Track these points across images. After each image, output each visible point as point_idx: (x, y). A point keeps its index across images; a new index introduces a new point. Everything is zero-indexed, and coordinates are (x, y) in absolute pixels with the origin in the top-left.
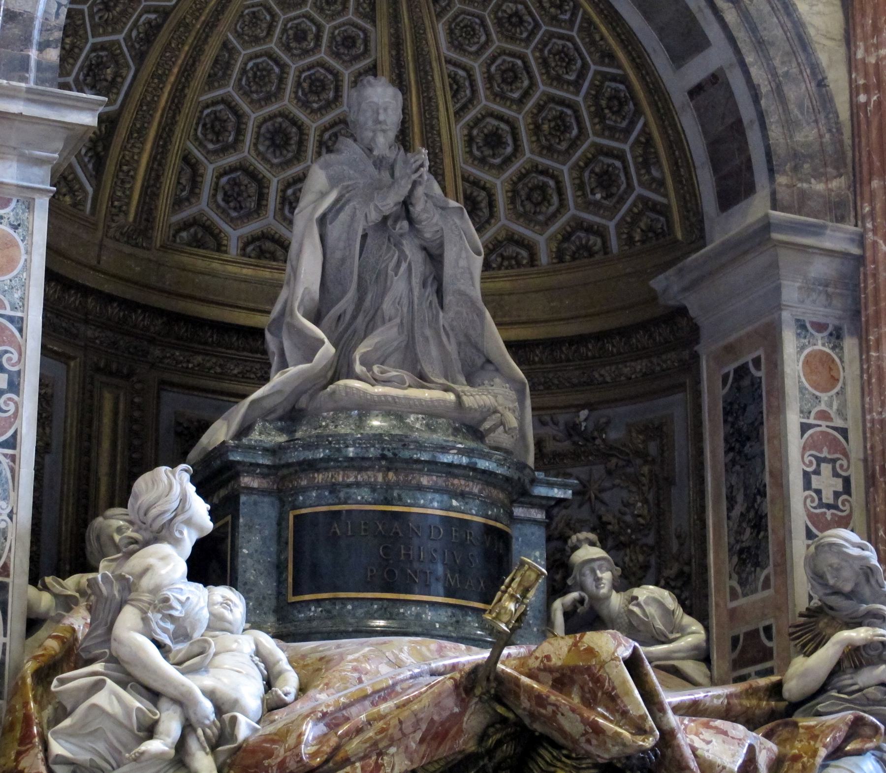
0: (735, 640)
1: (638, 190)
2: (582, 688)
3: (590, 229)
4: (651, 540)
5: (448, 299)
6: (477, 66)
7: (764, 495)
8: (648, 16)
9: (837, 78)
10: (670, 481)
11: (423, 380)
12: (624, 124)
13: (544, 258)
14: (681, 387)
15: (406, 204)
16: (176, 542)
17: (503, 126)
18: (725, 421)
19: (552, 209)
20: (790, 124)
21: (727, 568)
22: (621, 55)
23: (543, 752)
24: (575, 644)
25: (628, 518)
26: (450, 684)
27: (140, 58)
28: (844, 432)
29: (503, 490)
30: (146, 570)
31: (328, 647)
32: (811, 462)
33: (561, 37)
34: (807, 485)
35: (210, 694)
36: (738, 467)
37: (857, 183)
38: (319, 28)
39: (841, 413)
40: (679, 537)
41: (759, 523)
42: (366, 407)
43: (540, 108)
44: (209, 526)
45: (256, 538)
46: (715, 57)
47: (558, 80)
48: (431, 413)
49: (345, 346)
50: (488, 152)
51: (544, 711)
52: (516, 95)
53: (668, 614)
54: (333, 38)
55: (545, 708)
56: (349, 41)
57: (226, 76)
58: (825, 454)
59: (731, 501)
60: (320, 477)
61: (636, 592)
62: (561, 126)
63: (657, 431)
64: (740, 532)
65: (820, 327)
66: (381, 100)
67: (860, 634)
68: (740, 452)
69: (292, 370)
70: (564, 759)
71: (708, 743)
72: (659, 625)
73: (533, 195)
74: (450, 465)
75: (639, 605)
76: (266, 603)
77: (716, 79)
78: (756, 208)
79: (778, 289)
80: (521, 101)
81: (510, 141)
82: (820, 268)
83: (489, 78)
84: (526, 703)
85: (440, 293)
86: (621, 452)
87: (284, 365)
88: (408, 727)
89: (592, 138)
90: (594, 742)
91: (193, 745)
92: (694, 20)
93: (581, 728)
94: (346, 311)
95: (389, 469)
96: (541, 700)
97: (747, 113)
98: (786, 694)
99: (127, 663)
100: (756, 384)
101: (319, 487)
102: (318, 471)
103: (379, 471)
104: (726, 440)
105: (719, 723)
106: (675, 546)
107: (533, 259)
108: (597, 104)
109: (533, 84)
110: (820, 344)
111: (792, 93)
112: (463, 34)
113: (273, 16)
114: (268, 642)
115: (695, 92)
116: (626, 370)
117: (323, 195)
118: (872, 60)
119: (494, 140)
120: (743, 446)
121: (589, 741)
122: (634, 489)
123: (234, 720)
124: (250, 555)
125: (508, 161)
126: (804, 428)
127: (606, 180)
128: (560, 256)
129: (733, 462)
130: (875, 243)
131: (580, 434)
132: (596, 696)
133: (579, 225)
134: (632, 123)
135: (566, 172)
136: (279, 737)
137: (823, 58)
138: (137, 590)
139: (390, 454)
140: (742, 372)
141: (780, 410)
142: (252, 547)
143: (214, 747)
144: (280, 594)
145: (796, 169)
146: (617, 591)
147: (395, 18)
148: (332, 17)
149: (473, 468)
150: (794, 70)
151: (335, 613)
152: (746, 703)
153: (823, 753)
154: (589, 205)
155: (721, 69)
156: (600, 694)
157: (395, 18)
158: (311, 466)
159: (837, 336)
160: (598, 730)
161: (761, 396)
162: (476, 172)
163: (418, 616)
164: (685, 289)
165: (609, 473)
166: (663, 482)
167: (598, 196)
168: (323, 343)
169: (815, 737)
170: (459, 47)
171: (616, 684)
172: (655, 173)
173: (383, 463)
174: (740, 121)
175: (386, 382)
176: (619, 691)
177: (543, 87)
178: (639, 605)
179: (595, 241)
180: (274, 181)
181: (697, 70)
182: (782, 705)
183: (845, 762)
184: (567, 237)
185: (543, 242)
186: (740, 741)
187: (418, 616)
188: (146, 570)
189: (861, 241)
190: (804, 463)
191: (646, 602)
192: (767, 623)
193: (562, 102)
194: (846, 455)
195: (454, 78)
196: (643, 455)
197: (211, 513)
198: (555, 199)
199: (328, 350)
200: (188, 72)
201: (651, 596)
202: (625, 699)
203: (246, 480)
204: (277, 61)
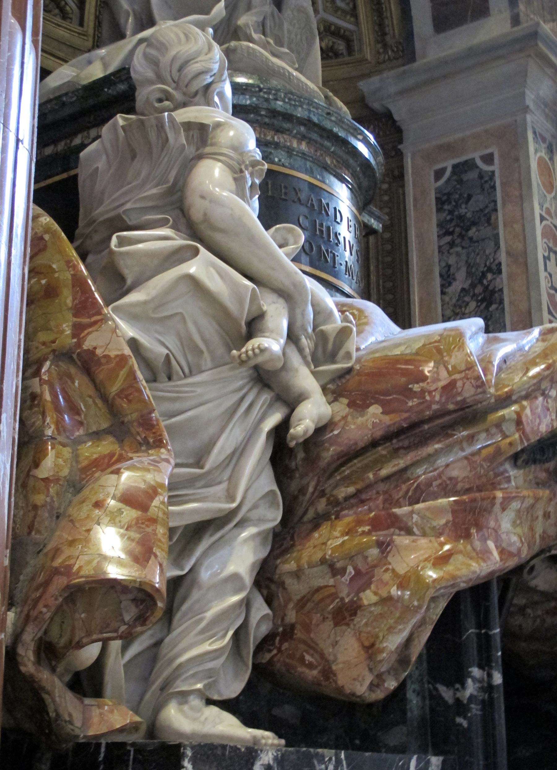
7: (500, 272)
18: (439, 210)
36: (459, 249)
59: (447, 278)
68: (462, 236)
99: (223, 231)
104: (440, 225)
120: (467, 230)
126: (542, 219)
129: (452, 244)
138: (212, 145)
139: (315, 119)
161: (494, 187)
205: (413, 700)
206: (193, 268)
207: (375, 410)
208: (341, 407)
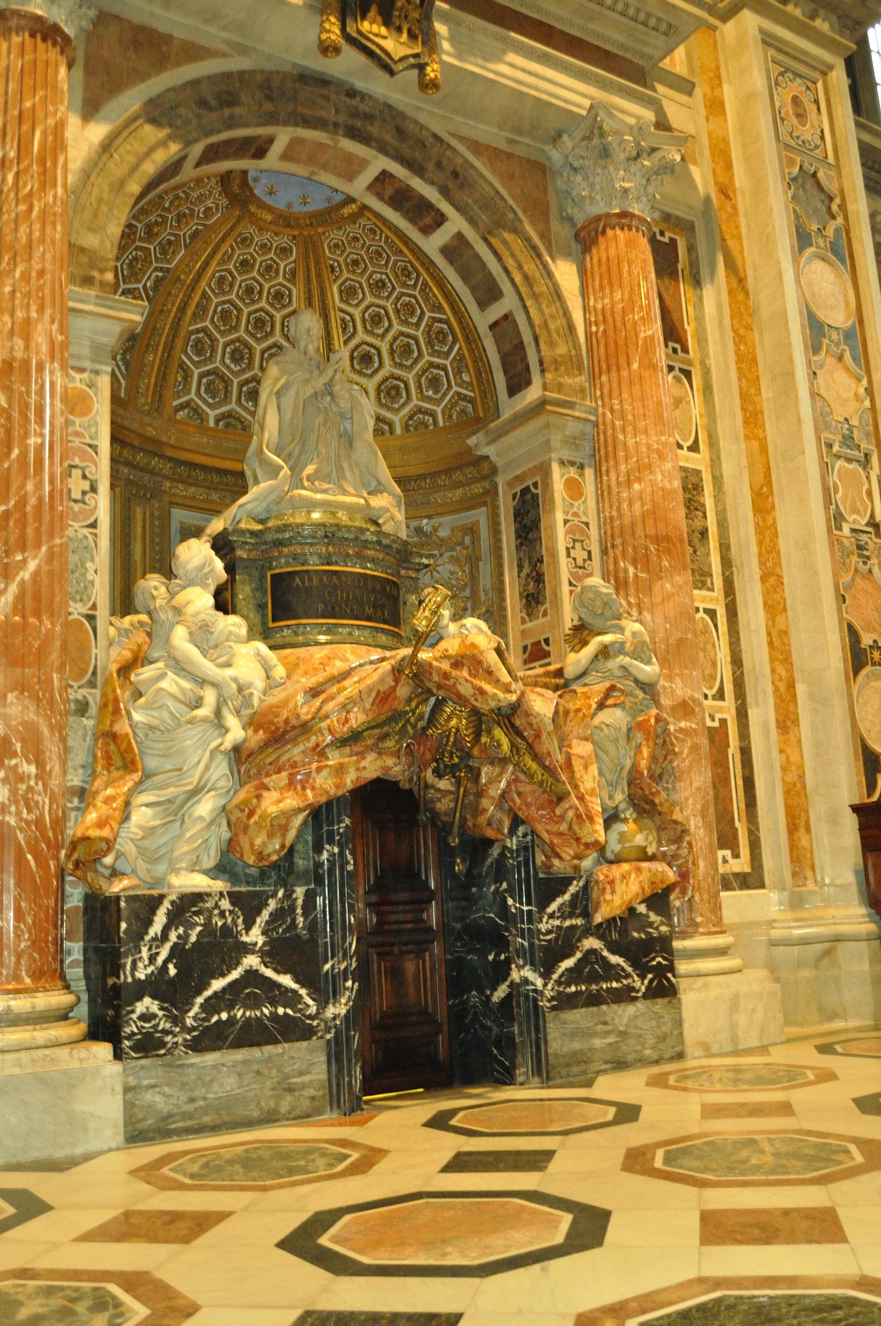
0: (525, 648)
1: (455, 388)
3: (426, 412)
4: (467, 593)
6: (357, 313)
8: (465, 278)
10: (479, 559)
11: (344, 492)
12: (446, 349)
13: (398, 430)
14: (485, 504)
15: (330, 384)
16: (205, 586)
17: (373, 351)
19: (402, 401)
21: (518, 606)
22: (445, 305)
26: (389, 667)
28: (587, 524)
30: (189, 603)
31: (302, 652)
33: (409, 295)
34: (569, 555)
35: (235, 680)
37: (592, 377)
38: (261, 285)
41: (539, 579)
42: (313, 505)
43: (395, 339)
44: (224, 576)
45: (248, 589)
46: (508, 303)
47: (406, 323)
48: (351, 509)
49: (296, 469)
52: (380, 331)
54: (269, 293)
56: (279, 296)
57: (205, 315)
58: (577, 537)
59: (520, 567)
60: (285, 550)
61: (464, 621)
62: (406, 350)
63: (472, 530)
64: (527, 585)
65: (572, 464)
66: (309, 323)
67: (608, 638)
69: (263, 485)
73: (389, 393)
74: (366, 541)
77: (507, 317)
78: (533, 393)
79: (548, 440)
80: (383, 336)
81: (376, 358)
82: (572, 428)
83: (364, 320)
84: (436, 678)
87: (257, 482)
88: (364, 696)
91: (225, 712)
92: (494, 280)
93: (472, 691)
94: (295, 450)
96: (446, 676)
97: (527, 337)
98: (566, 675)
100: (535, 497)
101: (286, 556)
105: (538, 690)
106: (482, 594)
107: (392, 431)
108: (429, 336)
109: (390, 325)
110: (573, 472)
111: (552, 326)
112: (348, 293)
113: (233, 277)
114: (262, 647)
115: (493, 327)
117: (277, 380)
118: (599, 306)
119: (366, 359)
123: (251, 694)
125: (375, 372)
126: (566, 522)
127: (434, 383)
128: (406, 427)
129: (521, 544)
130: (604, 414)
131: (425, 534)
133: (420, 410)
134: (451, 348)
135: (410, 377)
136: (285, 703)
140: (525, 491)
141: (552, 510)
142: (244, 592)
143: (238, 713)
144: (264, 623)
145: (556, 370)
147: (308, 281)
148: (269, 280)
149: (379, 542)
150: (554, 311)
152: (545, 680)
153: (594, 706)
154: (424, 398)
155: (511, 312)
157: (308, 281)
158: (279, 543)
159: (582, 467)
160: (482, 692)
163: (350, 634)
164: (489, 443)
166: (473, 560)
169: (589, 698)
170: (347, 302)
172: (466, 377)
174: (522, 343)
175: (324, 491)
177: (397, 327)
180: (236, 381)
181: (495, 312)
182: (562, 681)
183: (606, 711)
184: (411, 418)
186: (552, 700)
187: (350, 634)
188: (189, 603)
193: (409, 336)
195: (343, 320)
196: (461, 544)
197: (226, 568)
198: (404, 394)
199: (286, 471)
200: (183, 309)
204: (235, 306)
205: (300, 863)
206: (164, 684)
207: (261, 732)
208: (250, 732)
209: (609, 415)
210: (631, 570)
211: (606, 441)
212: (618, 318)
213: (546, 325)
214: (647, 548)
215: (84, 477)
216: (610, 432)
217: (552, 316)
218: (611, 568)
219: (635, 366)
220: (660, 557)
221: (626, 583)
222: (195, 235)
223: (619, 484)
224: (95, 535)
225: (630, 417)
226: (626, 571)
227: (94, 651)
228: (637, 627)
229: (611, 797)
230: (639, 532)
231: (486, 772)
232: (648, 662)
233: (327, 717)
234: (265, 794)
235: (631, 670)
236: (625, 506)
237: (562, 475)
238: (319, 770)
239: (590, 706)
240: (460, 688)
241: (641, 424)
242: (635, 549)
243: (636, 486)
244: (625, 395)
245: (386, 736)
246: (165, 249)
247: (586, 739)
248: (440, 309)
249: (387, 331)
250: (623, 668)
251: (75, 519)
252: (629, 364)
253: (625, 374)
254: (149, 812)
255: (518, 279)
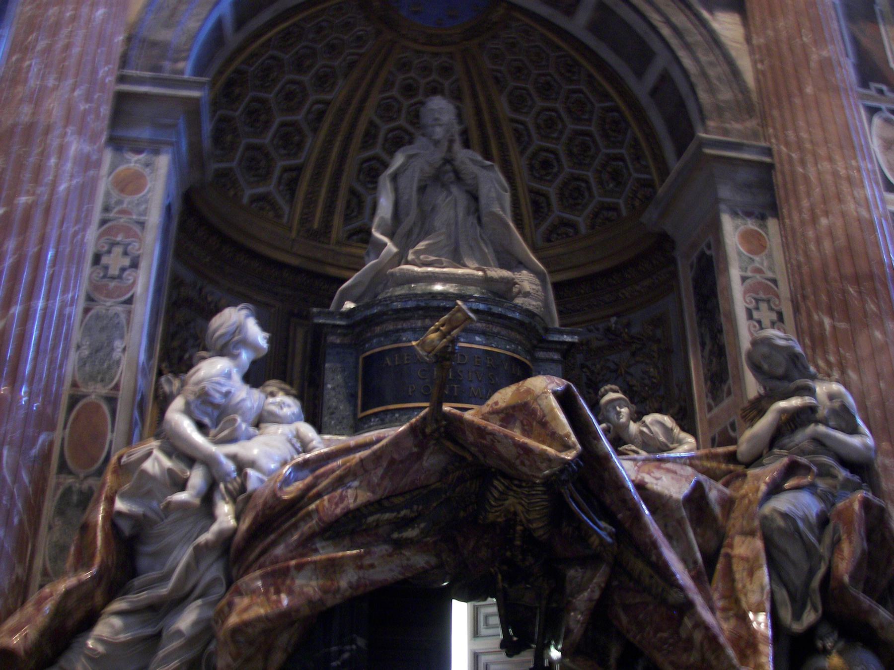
2: (522, 422)
5: (484, 219)
6: (529, 120)
9: (745, 64)
13: (583, 229)
15: (448, 161)
20: (712, 90)
21: (704, 390)
23: (496, 483)
24: (518, 389)
25: (647, 381)
27: (315, 130)
28: (774, 281)
29: (520, 333)
32: (751, 302)
34: (750, 317)
35: (234, 458)
39: (770, 269)
40: (677, 385)
43: (570, 140)
45: (339, 377)
50: (543, 172)
51: (484, 442)
53: (668, 431)
55: (485, 438)
58: (762, 295)
59: (703, 345)
60: (378, 329)
64: (711, 361)
66: (441, 110)
70: (515, 488)
71: (657, 479)
72: (662, 438)
75: (646, 426)
76: (345, 421)
81: (555, 163)
82: (744, 175)
83: (538, 127)
85: (479, 219)
86: (638, 339)
89: (604, 151)
90: (527, 463)
95: (425, 317)
97: (684, 89)
98: (739, 457)
102: (377, 324)
103: (418, 319)
110: (751, 225)
111: (711, 72)
112: (518, 102)
116: (638, 288)
119: (546, 165)
121: (522, 463)
122: (648, 361)
124: (333, 389)
125: (556, 175)
126: (744, 279)
127: (616, 176)
128: (593, 227)
132: (532, 426)
133: (604, 207)
135: (590, 175)
137: (733, 53)
141: (726, 270)
143: (233, 497)
146: (635, 422)
147: (475, 96)
151: (387, 420)
153: (763, 488)
156: (534, 424)
162: (536, 185)
165: (633, 354)
167: (611, 185)
168: (386, 245)
170: (516, 110)
171: (546, 411)
172: (643, 163)
173: (420, 312)
176: (548, 418)
178: (646, 426)
179: (612, 215)
181: (651, 77)
184: (596, 215)
185: (581, 220)
189: (769, 152)
190: (746, 302)
191: (651, 424)
192: (731, 420)
194: (778, 296)
195: (516, 130)
201: (657, 422)
202: (553, 424)
203: (332, 339)
209: (783, 149)
210: (827, 321)
211: (784, 180)
212: (785, 48)
213: (704, 74)
214: (844, 291)
215: (125, 253)
216: (787, 167)
217: (711, 64)
218: (805, 323)
219: (809, 90)
220: (863, 301)
221: (823, 339)
222: (352, 65)
223: (803, 223)
224: (129, 313)
225: (808, 146)
226: (821, 324)
227: (109, 437)
228: (836, 387)
229: (797, 616)
230: (833, 274)
231: (574, 573)
232: (853, 430)
233: (319, 495)
234: (237, 600)
235: (828, 442)
236: (812, 247)
237: (736, 227)
238: (300, 567)
239: (758, 490)
240: (500, 447)
241: (822, 152)
242: (830, 296)
243: (824, 221)
244: (801, 123)
245: (407, 523)
246: (324, 81)
247: (752, 533)
248: (606, 96)
249: (561, 133)
250: (819, 442)
251: (109, 295)
252: (801, 90)
253: (797, 101)
254: (117, 622)
255: (666, 31)
